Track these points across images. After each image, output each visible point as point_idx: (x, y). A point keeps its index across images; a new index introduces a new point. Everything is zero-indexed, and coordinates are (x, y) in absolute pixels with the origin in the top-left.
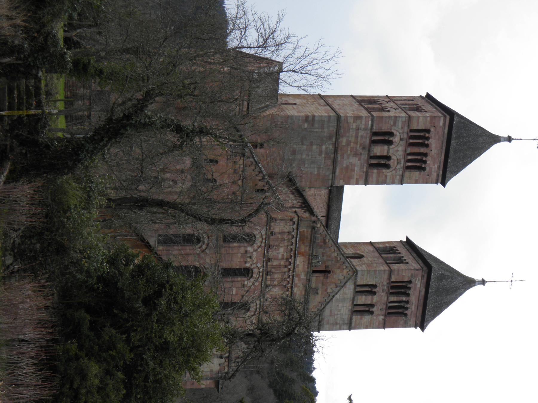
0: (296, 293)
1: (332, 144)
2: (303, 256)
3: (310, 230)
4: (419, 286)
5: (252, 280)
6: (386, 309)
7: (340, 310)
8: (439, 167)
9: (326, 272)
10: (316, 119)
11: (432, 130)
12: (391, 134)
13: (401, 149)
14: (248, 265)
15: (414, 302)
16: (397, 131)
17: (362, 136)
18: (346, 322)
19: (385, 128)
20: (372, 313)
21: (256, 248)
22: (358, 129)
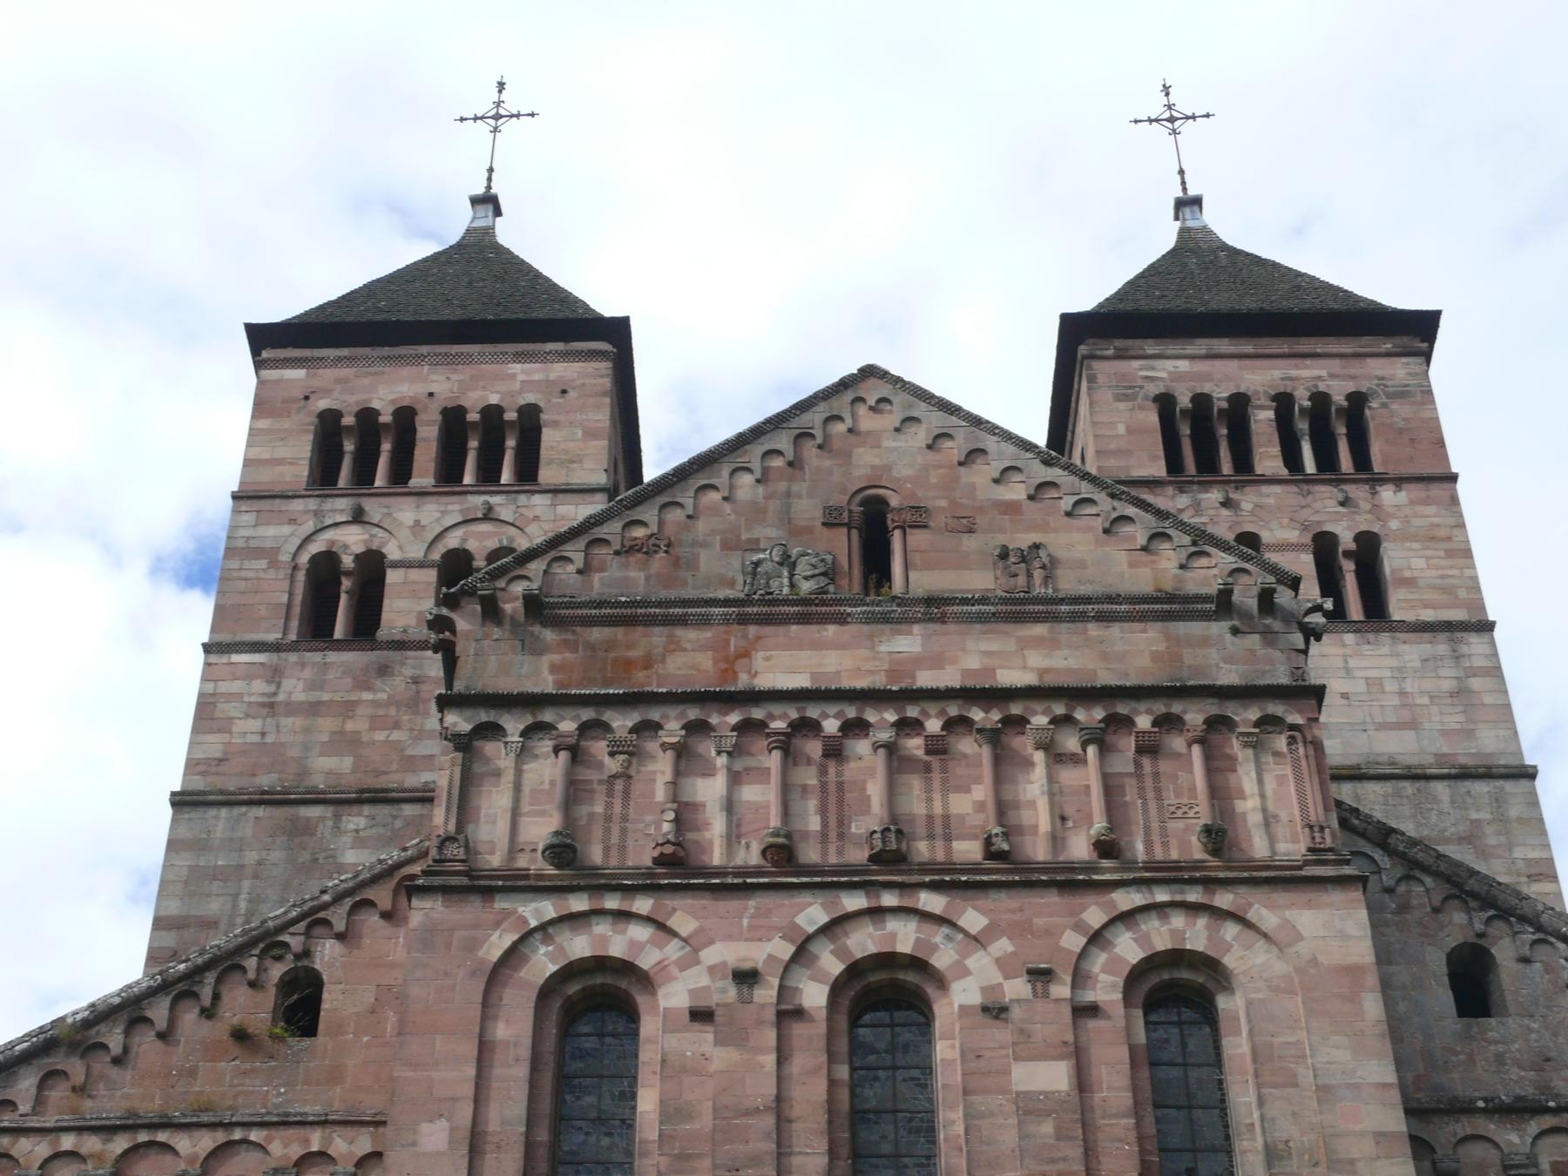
0: (1042, 672)
1: (337, 817)
2: (745, 654)
3: (549, 635)
4: (1183, 365)
5: (942, 959)
6: (1339, 481)
7: (1374, 684)
8: (520, 357)
9: (874, 526)
10: (174, 908)
11: (323, 404)
12: (324, 571)
13: (405, 512)
14: (814, 996)
15: (1277, 374)
16: (307, 540)
17: (313, 686)
19: (279, 593)
20: (1368, 546)
21: (673, 950)
22: (270, 707)
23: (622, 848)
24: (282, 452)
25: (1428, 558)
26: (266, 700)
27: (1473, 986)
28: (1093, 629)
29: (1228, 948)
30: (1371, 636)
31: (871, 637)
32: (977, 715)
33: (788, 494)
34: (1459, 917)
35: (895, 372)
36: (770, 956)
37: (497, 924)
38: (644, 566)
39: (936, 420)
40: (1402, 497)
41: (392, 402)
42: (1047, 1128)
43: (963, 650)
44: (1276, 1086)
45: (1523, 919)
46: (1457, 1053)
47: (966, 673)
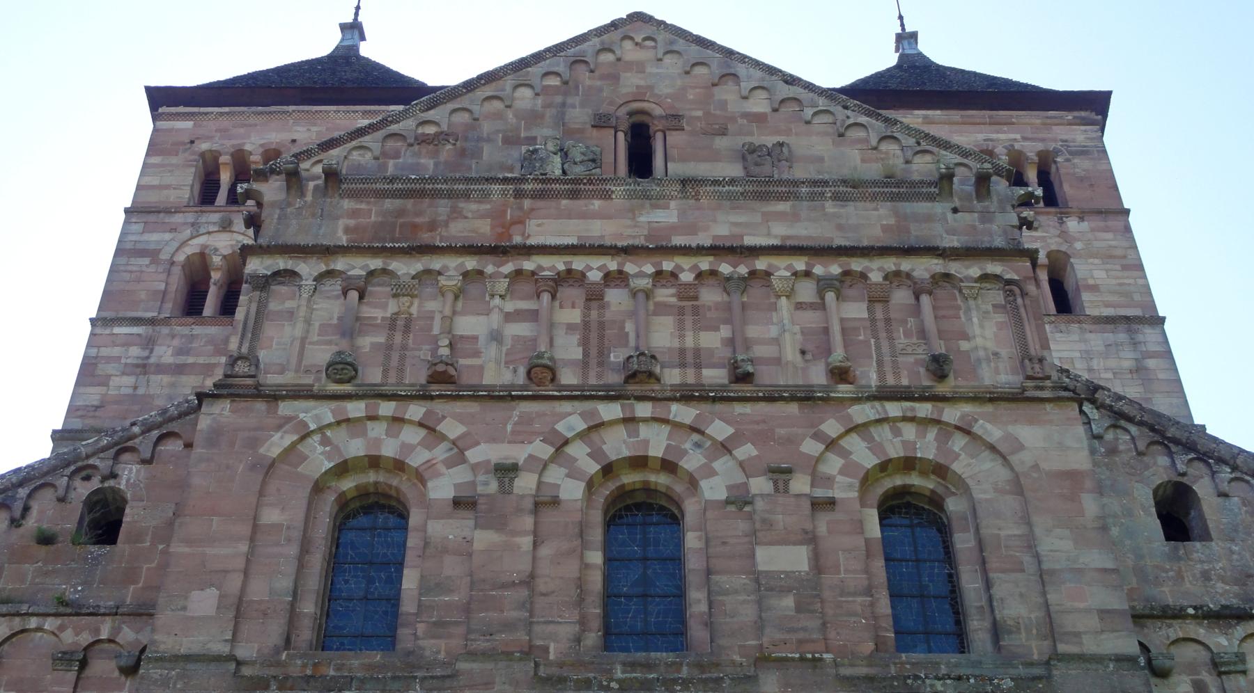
0: (784, 238)
2: (521, 222)
3: (347, 204)
5: (692, 461)
11: (204, 146)
14: (573, 491)
16: (184, 244)
17: (180, 352)
18: (1122, 337)
21: (441, 452)
23: (401, 370)
24: (169, 179)
25: (1107, 271)
26: (140, 362)
27: (1177, 516)
28: (830, 207)
29: (957, 456)
30: (1063, 327)
31: (632, 211)
32: (725, 269)
33: (564, 105)
34: (1163, 461)
35: (659, 17)
36: (531, 456)
37: (279, 427)
38: (435, 154)
39: (694, 51)
40: (1085, 225)
41: (262, 145)
42: (789, 602)
43: (715, 221)
44: (1003, 571)
45: (1221, 461)
46: (1167, 571)
47: (715, 237)
